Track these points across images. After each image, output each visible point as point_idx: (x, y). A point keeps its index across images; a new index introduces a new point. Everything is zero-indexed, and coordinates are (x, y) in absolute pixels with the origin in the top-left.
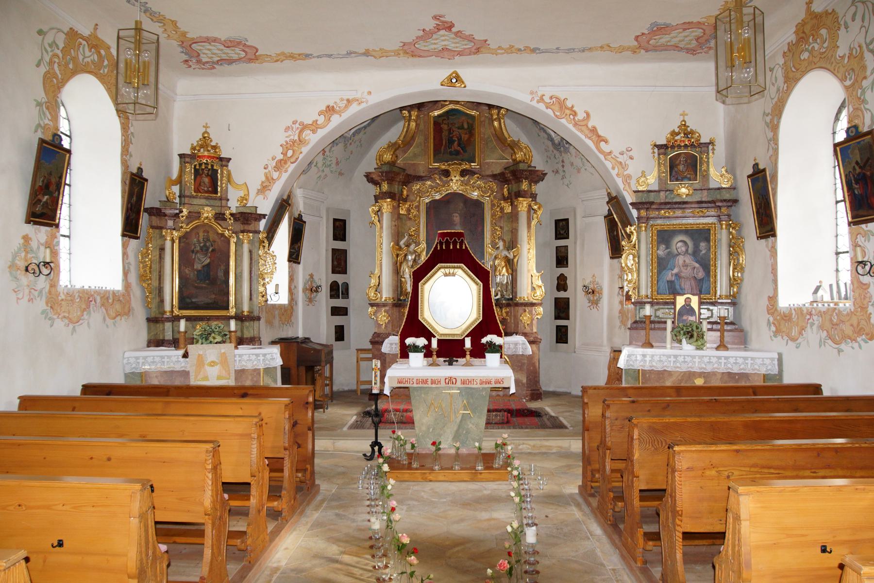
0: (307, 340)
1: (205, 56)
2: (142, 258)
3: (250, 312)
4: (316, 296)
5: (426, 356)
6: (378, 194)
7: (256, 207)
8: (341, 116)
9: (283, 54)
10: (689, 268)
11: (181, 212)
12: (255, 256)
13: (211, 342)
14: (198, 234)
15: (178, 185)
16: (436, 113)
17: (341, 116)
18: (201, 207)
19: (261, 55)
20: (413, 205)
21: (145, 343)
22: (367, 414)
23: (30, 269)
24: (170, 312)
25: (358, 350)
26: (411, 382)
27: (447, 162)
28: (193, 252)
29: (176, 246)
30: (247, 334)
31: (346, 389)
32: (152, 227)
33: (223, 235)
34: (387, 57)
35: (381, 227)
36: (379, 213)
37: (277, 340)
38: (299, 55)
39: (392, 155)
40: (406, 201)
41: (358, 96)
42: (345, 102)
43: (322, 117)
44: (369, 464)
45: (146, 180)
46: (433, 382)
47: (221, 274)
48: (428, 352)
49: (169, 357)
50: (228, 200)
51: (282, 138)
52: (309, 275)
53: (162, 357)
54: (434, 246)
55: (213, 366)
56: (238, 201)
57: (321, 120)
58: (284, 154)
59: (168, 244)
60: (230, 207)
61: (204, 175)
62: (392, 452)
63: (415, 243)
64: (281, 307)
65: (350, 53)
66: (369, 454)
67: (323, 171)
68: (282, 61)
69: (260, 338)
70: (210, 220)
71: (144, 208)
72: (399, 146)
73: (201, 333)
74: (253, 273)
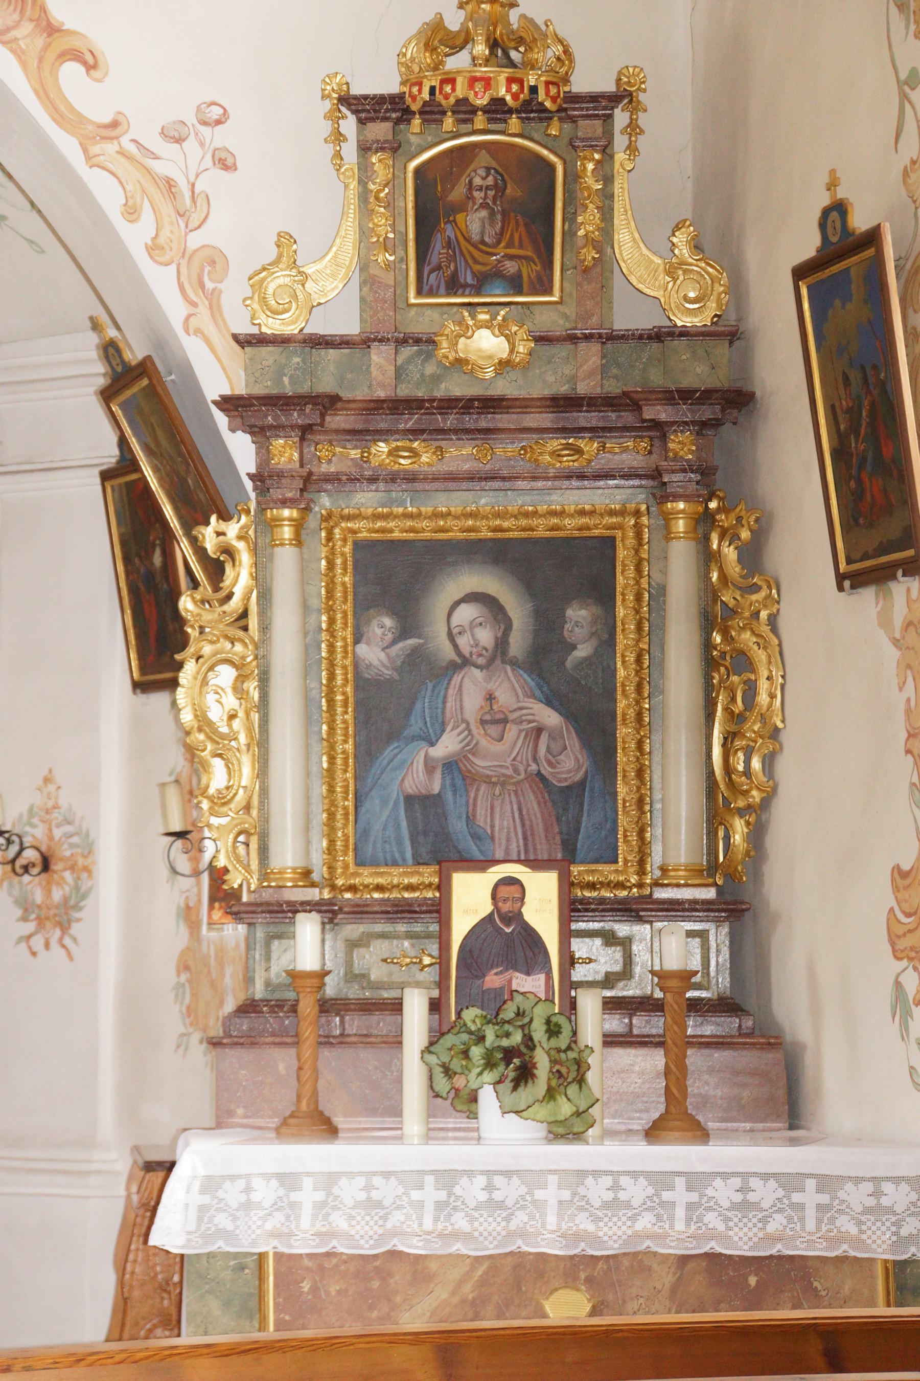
10: (512, 732)
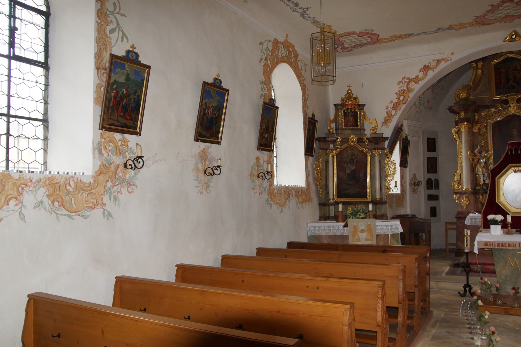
0: (414, 216)
1: (347, 44)
2: (316, 167)
3: (381, 198)
4: (418, 187)
5: (502, 227)
6: (457, 120)
7: (383, 133)
8: (434, 71)
9: (395, 36)
11: (337, 139)
12: (383, 164)
13: (358, 218)
14: (348, 152)
15: (335, 123)
16: (496, 61)
17: (434, 71)
18: (349, 135)
19: (380, 39)
20: (482, 125)
21: (318, 219)
22: (457, 265)
23: (260, 176)
24: (332, 199)
25: (446, 223)
26: (494, 245)
27: (506, 94)
28: (345, 163)
29: (335, 159)
30: (379, 213)
31: (438, 248)
32: (321, 149)
33: (362, 152)
34: (464, 28)
35: (461, 142)
36: (459, 132)
37: (395, 216)
38: (405, 35)
39: (466, 93)
40: (477, 123)
41: (445, 57)
42: (436, 61)
43: (422, 73)
44: (459, 298)
45: (317, 121)
46: (510, 245)
47: (362, 175)
48: (504, 225)
49: (333, 227)
50: (365, 130)
51: (396, 89)
52: (413, 175)
53: (329, 227)
54: (506, 152)
55: (362, 232)
56: (371, 130)
57: (421, 75)
58: (398, 99)
59: (330, 158)
60: (366, 134)
61: (350, 116)
62: (481, 293)
63: (486, 151)
64: (396, 195)
65: (438, 30)
66: (462, 293)
67: (419, 108)
68: (394, 41)
69: (387, 215)
70: (355, 143)
71: (316, 138)
72: (471, 87)
73: (352, 212)
74: (382, 175)
